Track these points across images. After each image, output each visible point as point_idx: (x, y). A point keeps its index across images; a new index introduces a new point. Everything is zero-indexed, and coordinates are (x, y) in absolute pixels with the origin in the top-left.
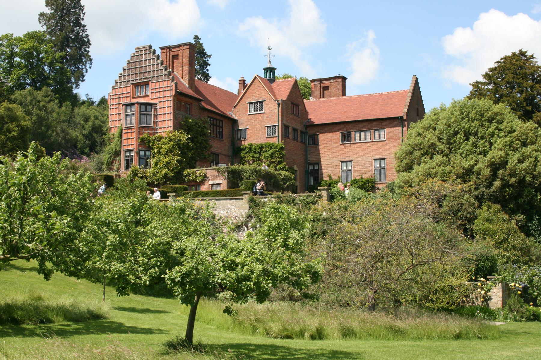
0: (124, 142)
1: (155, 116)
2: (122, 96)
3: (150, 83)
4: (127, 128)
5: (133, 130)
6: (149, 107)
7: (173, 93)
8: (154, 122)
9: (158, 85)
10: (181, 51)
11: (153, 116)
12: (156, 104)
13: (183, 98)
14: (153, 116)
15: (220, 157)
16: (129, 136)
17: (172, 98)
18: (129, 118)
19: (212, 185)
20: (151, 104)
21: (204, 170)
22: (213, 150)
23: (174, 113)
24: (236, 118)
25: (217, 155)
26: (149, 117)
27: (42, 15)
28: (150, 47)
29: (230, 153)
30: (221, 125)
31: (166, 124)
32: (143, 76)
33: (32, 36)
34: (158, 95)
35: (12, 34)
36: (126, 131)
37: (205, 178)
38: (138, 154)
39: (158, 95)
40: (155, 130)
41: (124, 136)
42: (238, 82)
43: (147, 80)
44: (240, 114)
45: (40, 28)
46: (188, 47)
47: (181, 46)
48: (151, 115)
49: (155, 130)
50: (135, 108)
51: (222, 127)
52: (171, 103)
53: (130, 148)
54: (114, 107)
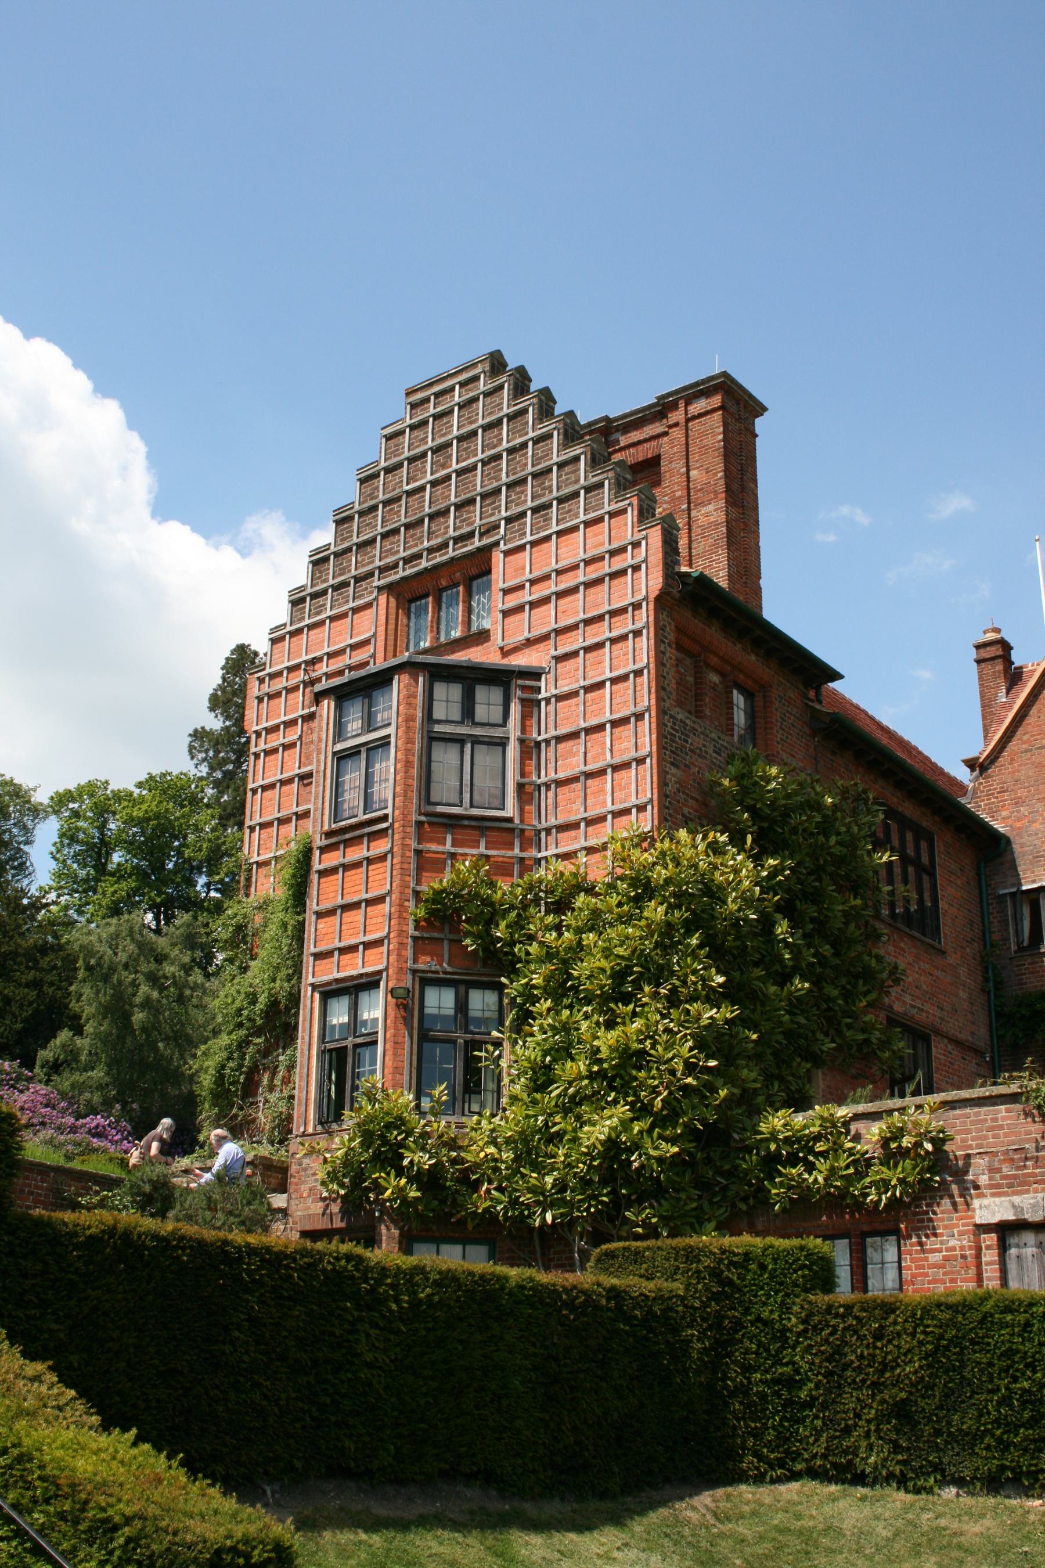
0: (322, 934)
1: (530, 749)
2: (323, 668)
3: (498, 558)
4: (341, 837)
5: (381, 846)
6: (488, 702)
7: (650, 582)
8: (520, 787)
9: (548, 558)
10: (678, 433)
11: (513, 751)
12: (535, 674)
13: (714, 634)
14: (513, 751)
15: (939, 1050)
16: (355, 886)
17: (645, 616)
18: (353, 776)
19: (1006, 1231)
20: (500, 678)
21: (919, 1113)
22: (902, 1001)
23: (662, 712)
24: (999, 826)
25: (920, 1036)
26: (486, 758)
27: (199, 735)
28: (496, 363)
29: (981, 1036)
30: (925, 859)
31: (604, 797)
32: (451, 526)
33: (162, 786)
34: (546, 619)
35: (107, 782)
36: (333, 859)
37: (938, 1174)
38: (406, 1005)
39: (546, 619)
40: (531, 839)
41: (325, 893)
42: (973, 654)
43: (476, 543)
44: (1018, 802)
45: (180, 763)
46: (716, 400)
47: (673, 406)
48: (502, 743)
49: (531, 839)
50: (395, 703)
51: (932, 875)
52: (642, 652)
53: (355, 967)
54: (277, 740)
